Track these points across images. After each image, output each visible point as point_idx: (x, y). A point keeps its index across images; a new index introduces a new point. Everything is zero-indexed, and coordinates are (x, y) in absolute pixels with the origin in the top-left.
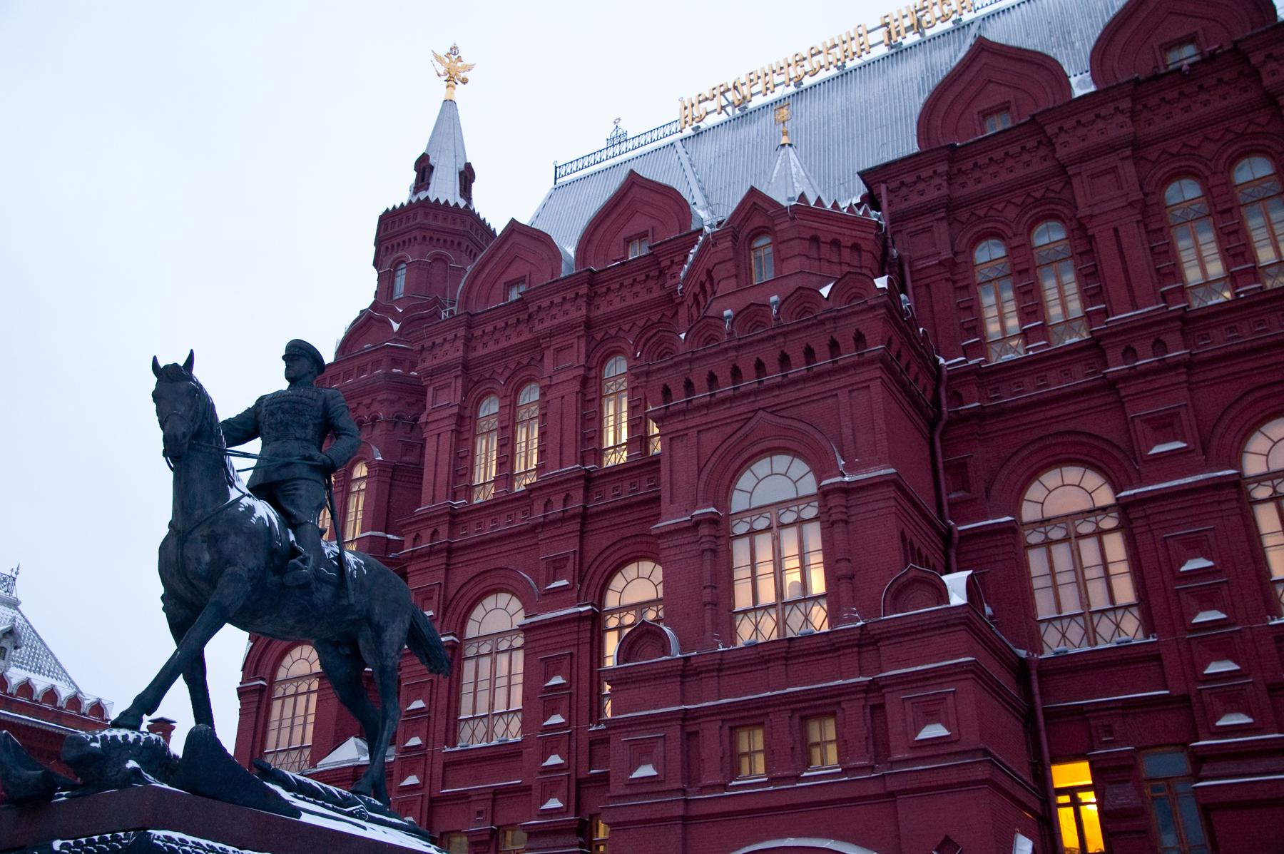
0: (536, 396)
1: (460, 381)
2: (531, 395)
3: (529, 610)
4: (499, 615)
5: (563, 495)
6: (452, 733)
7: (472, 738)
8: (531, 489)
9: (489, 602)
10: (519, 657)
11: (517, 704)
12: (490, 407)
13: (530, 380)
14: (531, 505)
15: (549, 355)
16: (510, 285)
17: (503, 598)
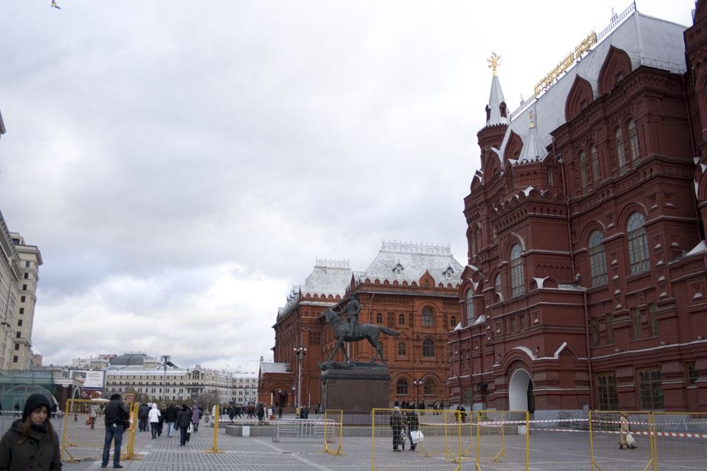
0: (634, 126)
1: (605, 126)
2: (632, 126)
3: (646, 218)
4: (636, 222)
5: (649, 169)
6: (628, 271)
7: (636, 271)
8: (639, 167)
9: (633, 217)
10: (645, 237)
11: (648, 257)
12: (619, 134)
13: (630, 119)
14: (639, 174)
15: (635, 106)
16: (617, 75)
17: (637, 214)
